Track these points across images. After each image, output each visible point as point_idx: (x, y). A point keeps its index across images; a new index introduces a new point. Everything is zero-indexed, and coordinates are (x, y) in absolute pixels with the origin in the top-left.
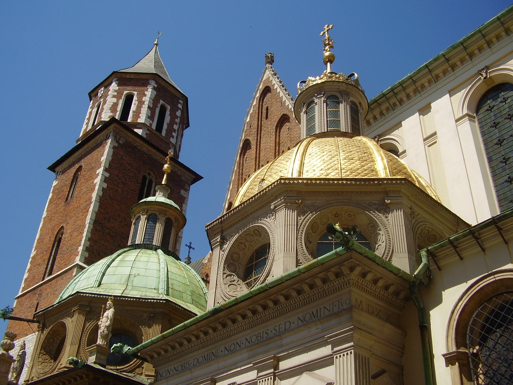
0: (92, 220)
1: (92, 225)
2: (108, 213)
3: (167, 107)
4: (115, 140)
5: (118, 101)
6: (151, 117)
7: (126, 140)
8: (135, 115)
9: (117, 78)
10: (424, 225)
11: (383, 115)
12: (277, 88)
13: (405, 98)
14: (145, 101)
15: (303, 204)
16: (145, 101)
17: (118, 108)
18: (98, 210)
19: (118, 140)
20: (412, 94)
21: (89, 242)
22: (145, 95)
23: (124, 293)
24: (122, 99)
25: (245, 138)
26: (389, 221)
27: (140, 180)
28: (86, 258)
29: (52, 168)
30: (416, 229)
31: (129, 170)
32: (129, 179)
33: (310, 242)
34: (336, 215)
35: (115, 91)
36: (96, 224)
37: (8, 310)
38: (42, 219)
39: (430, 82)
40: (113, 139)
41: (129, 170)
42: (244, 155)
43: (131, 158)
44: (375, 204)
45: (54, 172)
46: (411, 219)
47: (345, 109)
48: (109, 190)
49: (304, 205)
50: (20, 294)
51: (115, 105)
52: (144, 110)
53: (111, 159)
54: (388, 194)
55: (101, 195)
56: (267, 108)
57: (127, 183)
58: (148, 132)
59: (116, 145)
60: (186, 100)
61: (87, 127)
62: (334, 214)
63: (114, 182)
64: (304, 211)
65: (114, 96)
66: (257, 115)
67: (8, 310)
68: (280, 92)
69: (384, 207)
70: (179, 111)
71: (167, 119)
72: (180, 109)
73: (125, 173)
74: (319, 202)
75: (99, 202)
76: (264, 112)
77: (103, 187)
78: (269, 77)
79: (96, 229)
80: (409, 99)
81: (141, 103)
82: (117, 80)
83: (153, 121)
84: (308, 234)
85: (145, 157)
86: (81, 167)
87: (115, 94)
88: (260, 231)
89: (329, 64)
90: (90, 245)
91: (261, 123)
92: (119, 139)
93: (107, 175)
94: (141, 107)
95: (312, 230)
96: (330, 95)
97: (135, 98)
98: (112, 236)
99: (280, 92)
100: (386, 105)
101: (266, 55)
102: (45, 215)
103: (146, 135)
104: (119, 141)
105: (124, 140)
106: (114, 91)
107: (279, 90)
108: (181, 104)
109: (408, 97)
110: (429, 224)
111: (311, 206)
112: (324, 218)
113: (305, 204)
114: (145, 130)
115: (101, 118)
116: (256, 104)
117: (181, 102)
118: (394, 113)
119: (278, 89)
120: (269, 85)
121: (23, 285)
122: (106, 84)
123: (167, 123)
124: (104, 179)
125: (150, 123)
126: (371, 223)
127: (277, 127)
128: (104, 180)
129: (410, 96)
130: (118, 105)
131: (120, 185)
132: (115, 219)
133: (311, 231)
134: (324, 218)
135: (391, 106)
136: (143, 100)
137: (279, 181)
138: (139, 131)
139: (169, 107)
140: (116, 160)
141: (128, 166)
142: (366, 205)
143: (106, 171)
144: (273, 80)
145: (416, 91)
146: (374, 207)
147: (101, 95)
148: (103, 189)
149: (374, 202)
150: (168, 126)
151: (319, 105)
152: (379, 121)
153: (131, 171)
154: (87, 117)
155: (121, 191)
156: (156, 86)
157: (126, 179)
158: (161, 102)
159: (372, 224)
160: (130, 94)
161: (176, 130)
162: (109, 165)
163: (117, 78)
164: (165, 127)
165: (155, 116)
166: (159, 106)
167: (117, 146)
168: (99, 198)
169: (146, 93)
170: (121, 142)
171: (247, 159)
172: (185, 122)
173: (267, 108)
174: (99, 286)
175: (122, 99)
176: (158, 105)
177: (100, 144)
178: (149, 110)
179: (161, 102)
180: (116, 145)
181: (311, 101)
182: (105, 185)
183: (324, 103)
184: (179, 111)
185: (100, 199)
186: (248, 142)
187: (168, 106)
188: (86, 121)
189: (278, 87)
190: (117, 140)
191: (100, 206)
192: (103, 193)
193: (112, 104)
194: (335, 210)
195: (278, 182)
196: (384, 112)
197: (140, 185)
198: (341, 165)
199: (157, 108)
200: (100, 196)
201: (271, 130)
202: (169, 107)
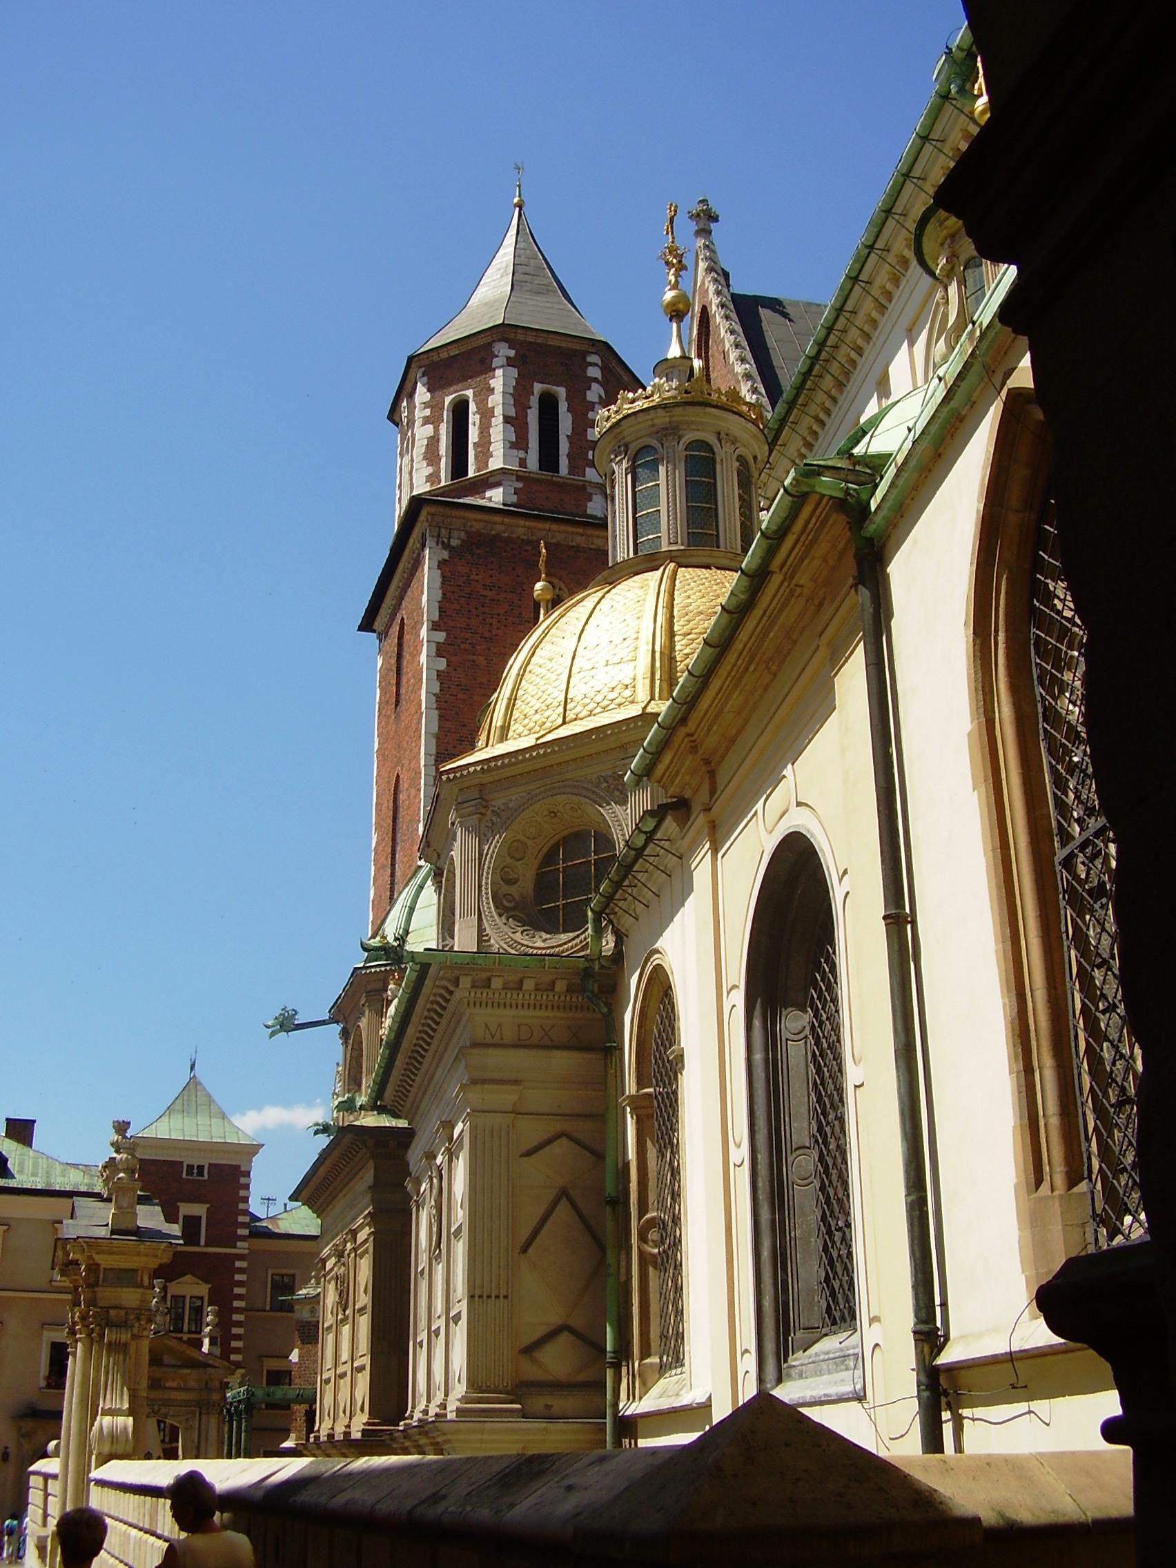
0: (431, 755)
2: (464, 726)
3: (556, 392)
4: (438, 545)
5: (436, 429)
6: (518, 443)
7: (466, 532)
8: (480, 452)
9: (423, 369)
13: (853, 355)
14: (493, 407)
16: (493, 407)
18: (439, 728)
19: (446, 540)
22: (492, 391)
24: (445, 421)
29: (367, 625)
31: (494, 600)
33: (510, 882)
34: (553, 815)
35: (426, 405)
37: (286, 1014)
40: (434, 544)
41: (494, 600)
45: (374, 631)
48: (455, 670)
49: (493, 811)
51: (433, 441)
52: (498, 431)
53: (441, 595)
55: (437, 690)
57: (496, 635)
58: (520, 485)
59: (445, 555)
60: (605, 349)
63: (463, 646)
65: (426, 421)
67: (286, 1014)
70: (595, 387)
71: (566, 423)
72: (595, 380)
73: (484, 613)
75: (437, 708)
77: (438, 671)
81: (487, 414)
82: (424, 374)
85: (527, 551)
86: (402, 619)
87: (428, 412)
92: (449, 538)
93: (441, 636)
94: (489, 426)
97: (472, 407)
101: (689, 213)
103: (515, 493)
104: (449, 541)
105: (463, 535)
106: (423, 405)
108: (596, 365)
109: (860, 351)
114: (511, 483)
123: (568, 436)
124: (435, 650)
125: (520, 459)
128: (436, 653)
130: (438, 440)
131: (477, 647)
133: (509, 860)
136: (490, 405)
138: (496, 497)
139: (561, 392)
140: (453, 592)
143: (436, 630)
150: (570, 443)
153: (498, 601)
155: (486, 659)
156: (512, 353)
157: (491, 624)
158: (538, 387)
160: (458, 399)
162: (440, 611)
163: (423, 369)
164: (564, 447)
166: (534, 401)
169: (493, 383)
170: (454, 542)
175: (445, 421)
176: (529, 400)
177: (417, 563)
179: (538, 387)
180: (445, 555)
182: (442, 664)
184: (595, 386)
185: (437, 701)
190: (443, 542)
192: (441, 683)
193: (425, 442)
196: (833, 392)
199: (529, 411)
200: (435, 695)
202: (561, 392)
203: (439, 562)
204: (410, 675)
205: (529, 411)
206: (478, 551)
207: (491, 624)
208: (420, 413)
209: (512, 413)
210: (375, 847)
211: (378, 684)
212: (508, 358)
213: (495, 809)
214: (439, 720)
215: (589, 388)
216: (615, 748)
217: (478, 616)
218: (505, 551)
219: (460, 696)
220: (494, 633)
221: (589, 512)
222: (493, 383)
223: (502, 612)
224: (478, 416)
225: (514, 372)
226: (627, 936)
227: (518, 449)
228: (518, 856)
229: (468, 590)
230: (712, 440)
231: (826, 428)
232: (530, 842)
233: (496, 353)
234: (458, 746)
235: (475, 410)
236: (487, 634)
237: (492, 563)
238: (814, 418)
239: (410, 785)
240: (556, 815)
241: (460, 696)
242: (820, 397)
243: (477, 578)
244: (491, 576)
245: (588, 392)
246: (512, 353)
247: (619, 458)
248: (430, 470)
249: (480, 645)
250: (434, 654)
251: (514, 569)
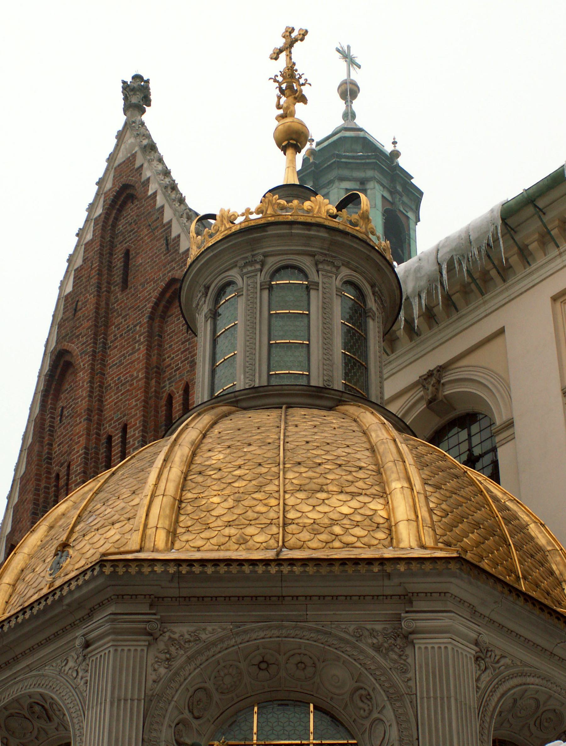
10: (521, 685)
11: (453, 309)
12: (155, 194)
13: (515, 260)
15: (167, 634)
20: (533, 246)
25: (59, 347)
26: (411, 683)
30: (493, 704)
34: (263, 666)
42: (56, 398)
44: (373, 633)
46: (479, 672)
47: (326, 308)
49: (170, 638)
54: (411, 602)
56: (127, 253)
62: (256, 661)
64: (168, 656)
66: (94, 273)
68: (163, 207)
69: (399, 641)
74: (213, 630)
76: (119, 264)
78: (134, 156)
80: (528, 263)
84: (178, 724)
88: (47, 706)
91: (108, 299)
95: (191, 711)
96: (283, 263)
99: (163, 207)
107: (160, 200)
110: (537, 681)
111: (189, 641)
112: (225, 675)
113: (173, 636)
116: (92, 241)
118: (485, 303)
119: (158, 198)
120: (132, 180)
126: (362, 688)
127: (151, 318)
129: (531, 254)
133: (187, 714)
134: (225, 675)
135: (474, 280)
137: (97, 568)
142: (348, 637)
144: (146, 165)
146: (370, 641)
149: (369, 627)
151: (248, 295)
152: (442, 326)
159: (363, 692)
171: (65, 413)
173: (127, 253)
181: (227, 279)
183: (261, 290)
186: (67, 358)
189: (159, 192)
194: (257, 652)
195: (96, 573)
198: (287, 508)
201: (135, 326)
213: (176, 636)
216: (391, 596)
228: (196, 714)
230: (367, 289)
232: (216, 697)
247: (250, 269)
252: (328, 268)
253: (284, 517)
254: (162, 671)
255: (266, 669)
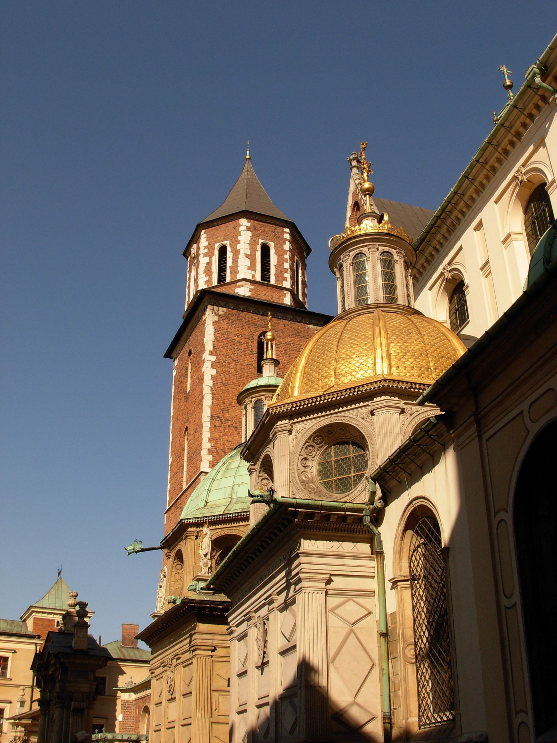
1: (209, 423)
2: (224, 403)
3: (270, 244)
6: (252, 267)
13: (460, 216)
14: (240, 250)
16: (240, 250)
17: (212, 268)
19: (216, 311)
21: (210, 444)
22: (239, 242)
23: (228, 509)
27: (255, 350)
28: (210, 462)
32: (241, 353)
34: (330, 432)
35: (206, 247)
36: (213, 420)
38: (171, 419)
39: (478, 192)
40: (211, 313)
43: (238, 327)
45: (172, 358)
48: (220, 375)
50: (167, 508)
51: (209, 264)
57: (240, 359)
58: (252, 287)
59: (216, 318)
61: (189, 298)
65: (205, 255)
70: (288, 243)
71: (273, 259)
72: (287, 240)
73: (234, 348)
79: (215, 426)
81: (236, 253)
82: (204, 233)
83: (255, 270)
85: (255, 319)
87: (206, 251)
89: (368, 196)
90: (212, 446)
93: (213, 358)
94: (237, 258)
97: (229, 249)
98: (236, 427)
100: (444, 228)
102: (172, 414)
103: (250, 291)
114: (248, 286)
115: (197, 286)
117: (287, 230)
121: (168, 499)
122: (195, 239)
123: (275, 266)
125: (253, 275)
131: (231, 364)
132: (234, 406)
139: (272, 245)
141: (236, 338)
143: (211, 355)
145: (468, 207)
147: (193, 255)
148: (212, 377)
150: (276, 269)
153: (241, 343)
154: (187, 285)
156: (249, 224)
157: (238, 354)
161: (287, 269)
165: (256, 263)
166: (259, 248)
167: (217, 320)
168: (210, 389)
169: (239, 238)
172: (304, 248)
174: (205, 506)
178: (247, 258)
182: (214, 372)
185: (211, 390)
187: (270, 243)
188: (187, 290)
190: (215, 313)
191: (213, 398)
192: (214, 381)
193: (205, 265)
196: (446, 235)
197: (257, 355)
199: (256, 252)
200: (210, 387)
203: (213, 322)
204: (195, 377)
205: (256, 252)
206: (232, 318)
207: (238, 354)
208: (203, 251)
209: (249, 252)
210: (171, 463)
211: (173, 383)
212: (247, 227)
213: (298, 429)
214: (212, 400)
215: (285, 244)
217: (231, 349)
218: (245, 319)
219: (223, 388)
220: (239, 358)
221: (285, 302)
222: (239, 238)
223: (243, 348)
224: (232, 254)
225: (250, 234)
226: (390, 493)
227: (252, 270)
229: (226, 336)
231: (440, 253)
233: (241, 224)
234: (221, 413)
235: (231, 250)
236: (235, 358)
237: (239, 324)
238: (433, 247)
239: (195, 432)
240: (331, 433)
241: (223, 388)
242: (439, 237)
243: (231, 331)
244: (238, 331)
245: (284, 245)
246: (249, 224)
248: (207, 278)
249: (233, 364)
250: (210, 367)
251: (249, 328)
252: (373, 250)
253: (335, 372)
254: (295, 442)
255: (331, 433)
